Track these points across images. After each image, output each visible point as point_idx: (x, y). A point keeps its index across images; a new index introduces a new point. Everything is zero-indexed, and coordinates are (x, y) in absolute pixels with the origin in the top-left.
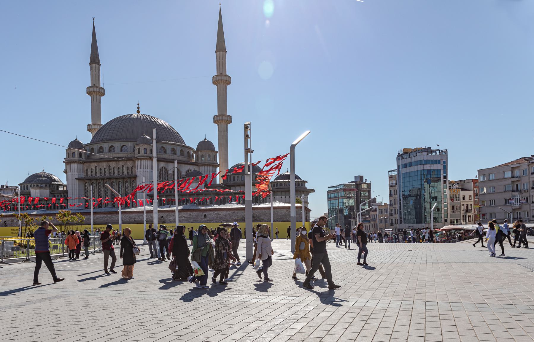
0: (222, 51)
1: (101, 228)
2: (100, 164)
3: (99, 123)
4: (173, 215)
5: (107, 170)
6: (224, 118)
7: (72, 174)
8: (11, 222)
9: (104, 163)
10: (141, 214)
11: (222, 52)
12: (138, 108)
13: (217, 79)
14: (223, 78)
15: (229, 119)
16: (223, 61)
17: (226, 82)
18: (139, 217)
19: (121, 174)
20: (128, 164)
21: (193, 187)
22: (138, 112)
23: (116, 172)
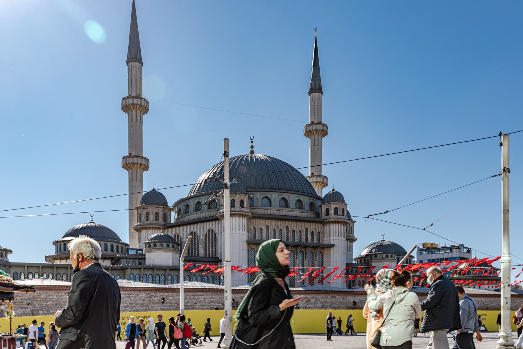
0: (318, 92)
1: (482, 315)
2: (274, 222)
3: (141, 155)
4: (515, 301)
5: (284, 231)
6: (319, 180)
7: (240, 234)
8: (306, 301)
9: (280, 223)
10: (497, 299)
11: (317, 93)
12: (252, 147)
13: (318, 128)
14: (319, 127)
15: (325, 181)
16: (314, 105)
17: (322, 132)
18: (478, 302)
19: (303, 241)
20: (312, 227)
21: (392, 267)
22: (252, 152)
23: (297, 238)
